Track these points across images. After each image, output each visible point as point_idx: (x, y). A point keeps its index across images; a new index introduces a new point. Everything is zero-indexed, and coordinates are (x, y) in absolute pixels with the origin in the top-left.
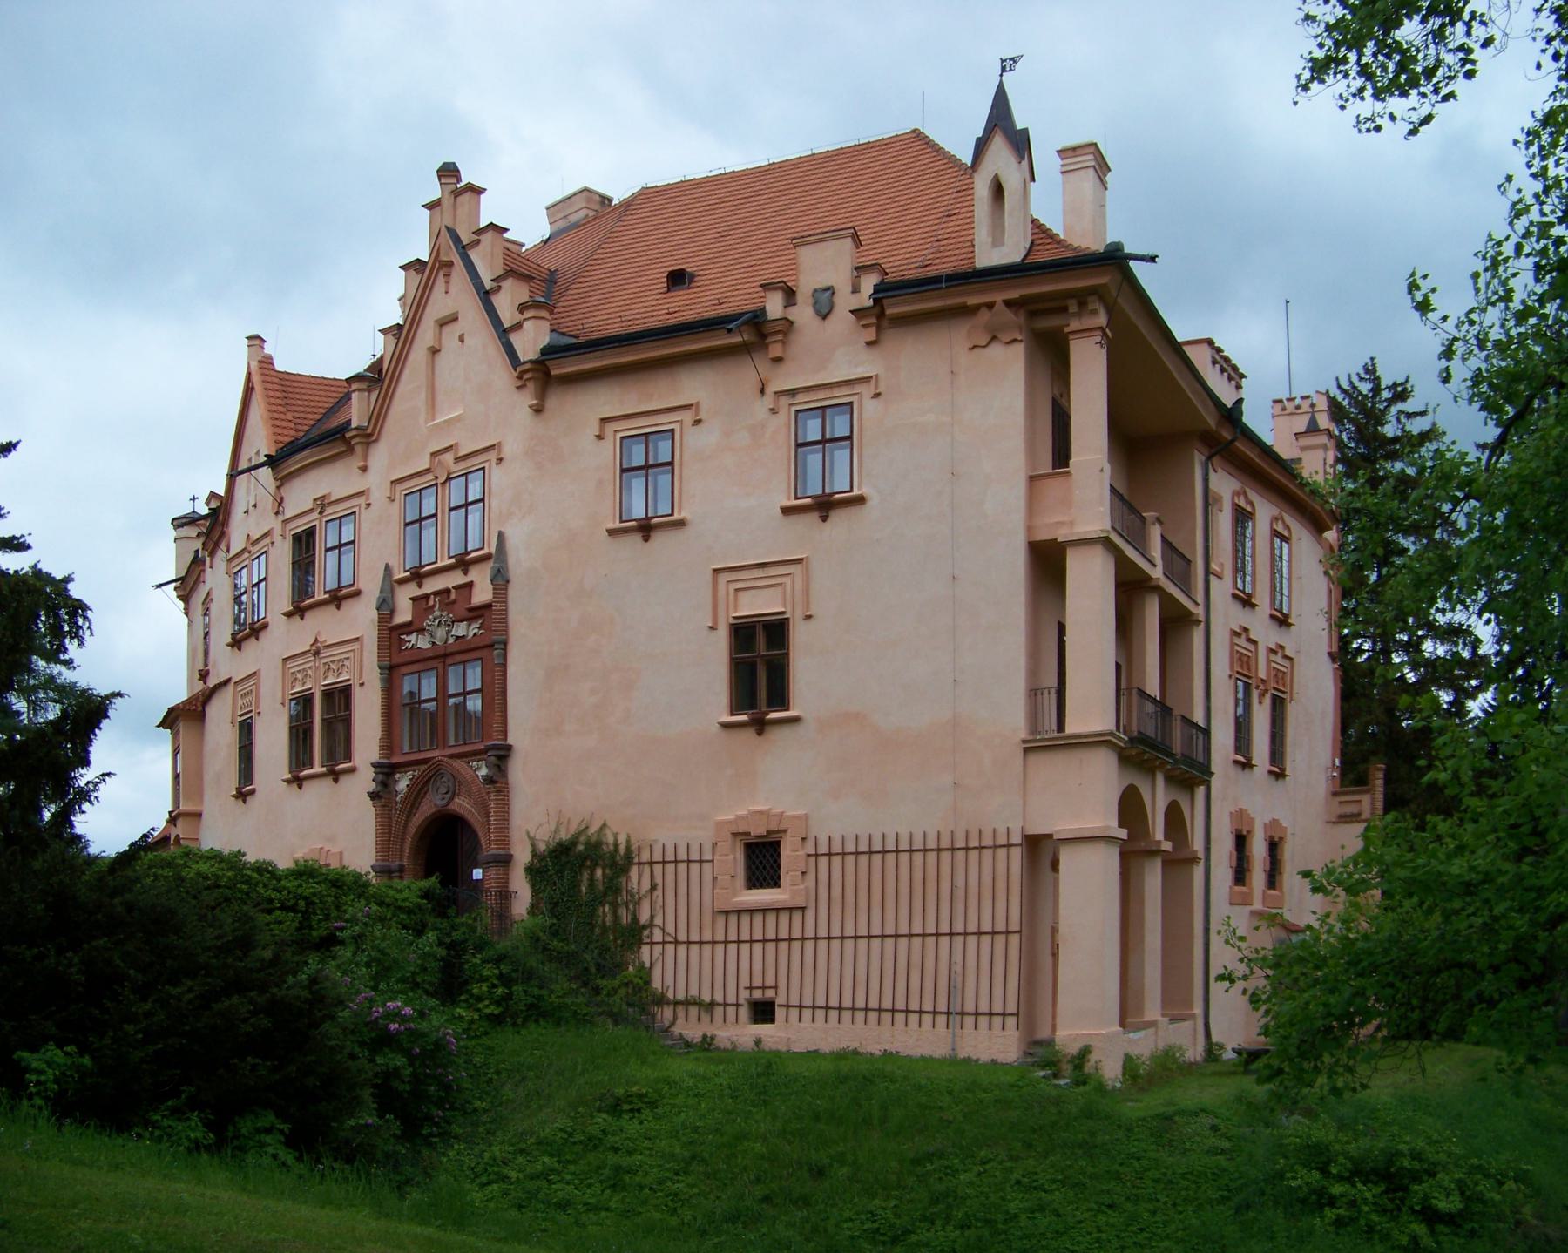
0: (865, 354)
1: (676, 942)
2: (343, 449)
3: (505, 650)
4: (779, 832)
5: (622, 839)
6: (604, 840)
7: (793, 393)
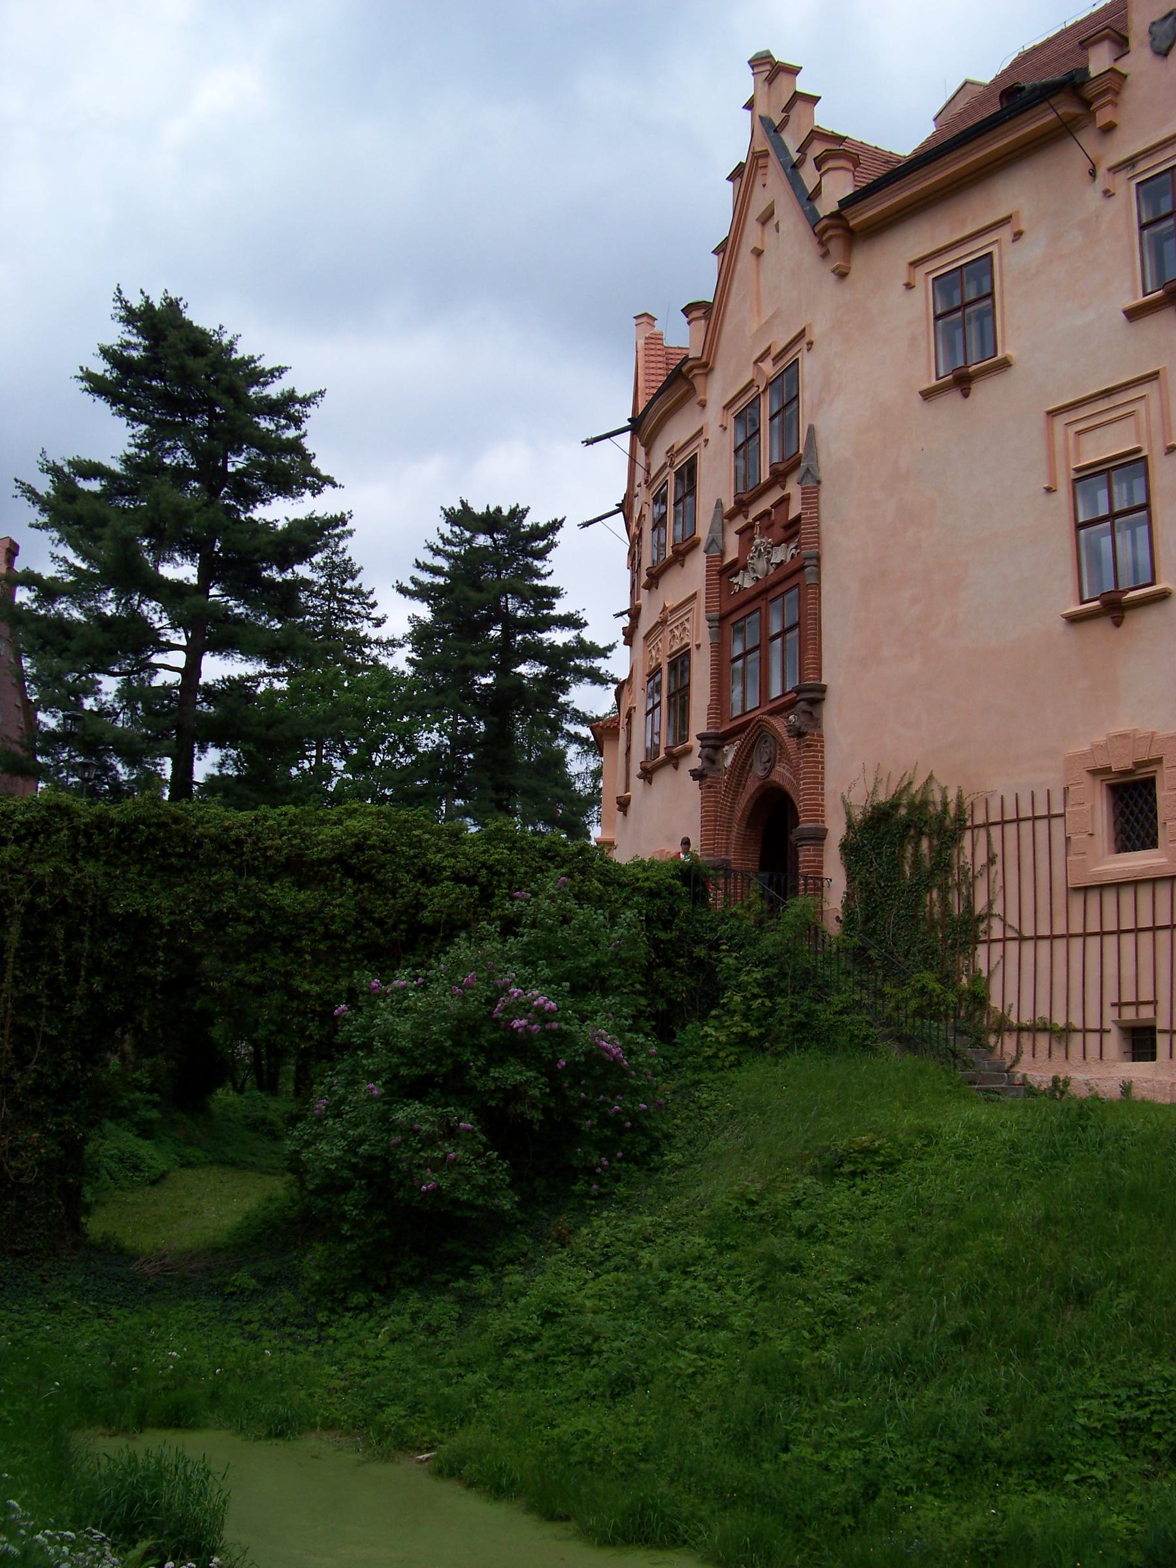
1: (1021, 939)
3: (818, 566)
4: (1150, 762)
5: (952, 796)
6: (931, 799)
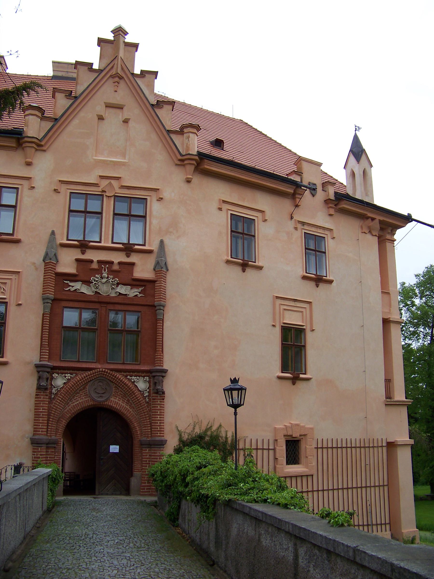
0: (328, 218)
2: (14, 145)
6: (221, 435)
7: (303, 223)
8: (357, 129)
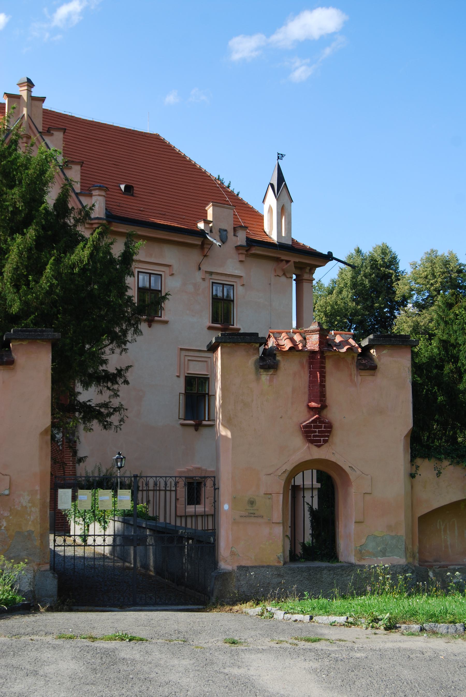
7: (211, 273)
8: (280, 156)
